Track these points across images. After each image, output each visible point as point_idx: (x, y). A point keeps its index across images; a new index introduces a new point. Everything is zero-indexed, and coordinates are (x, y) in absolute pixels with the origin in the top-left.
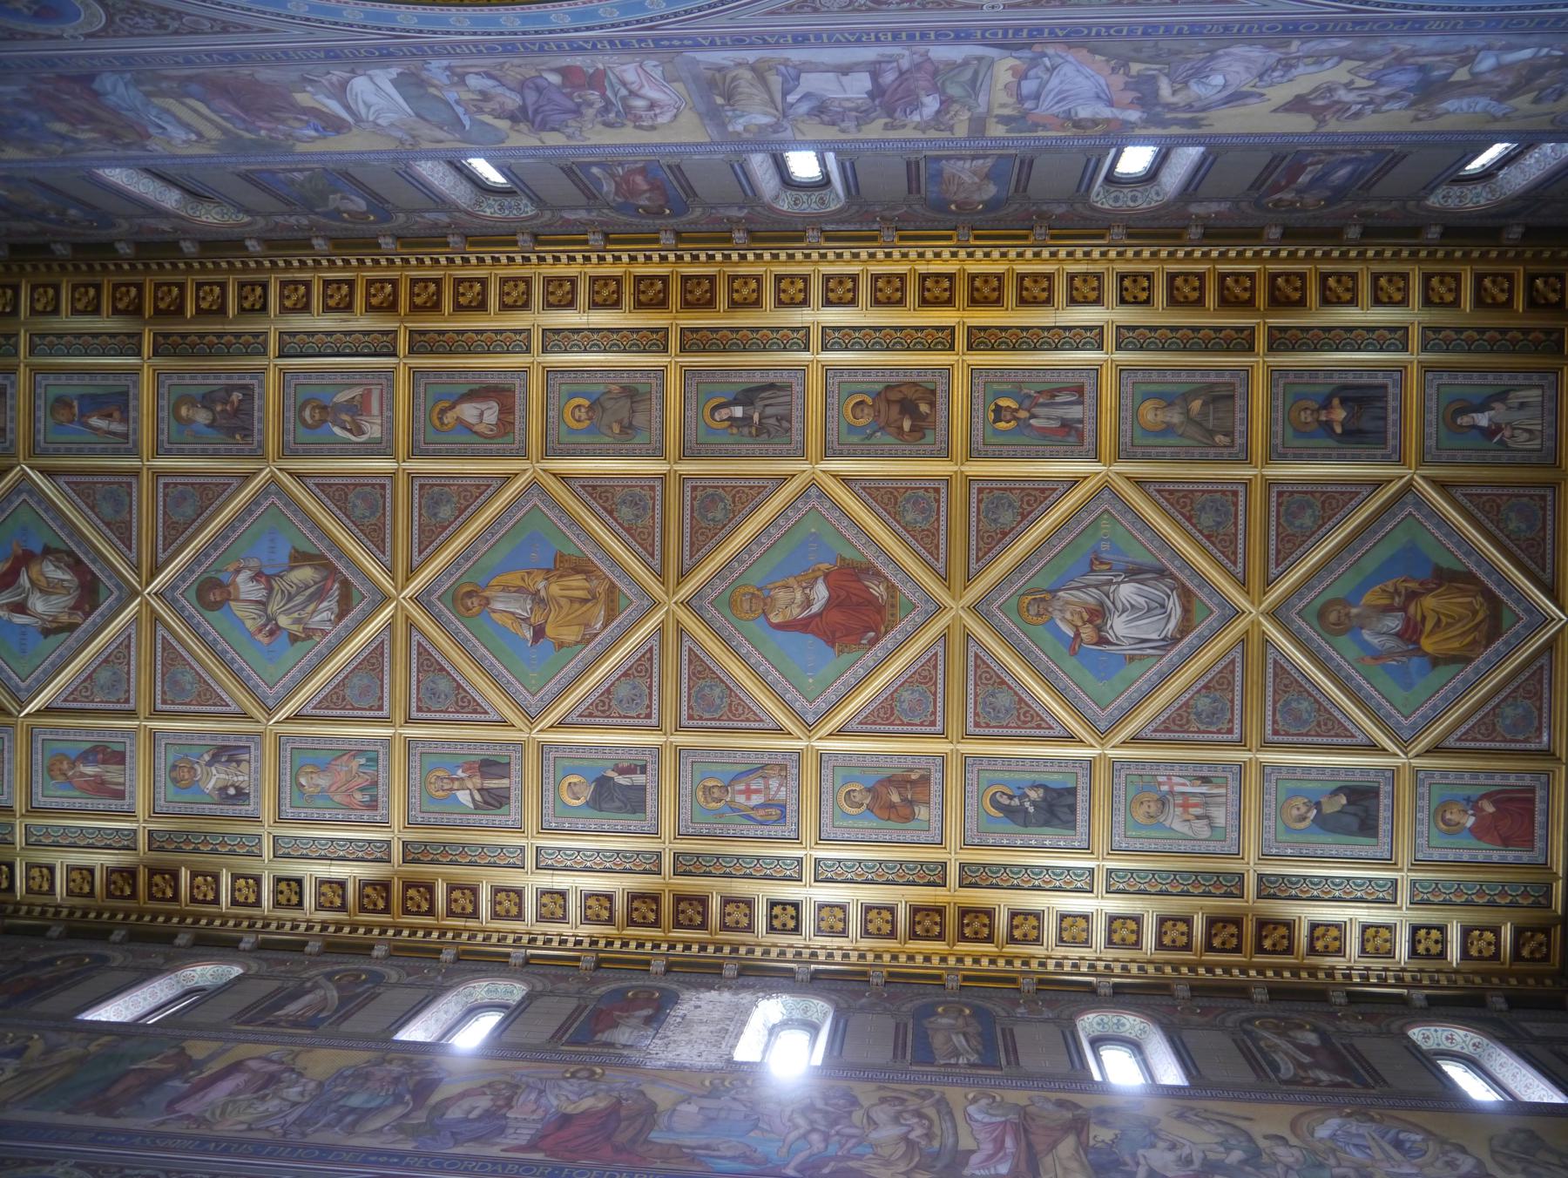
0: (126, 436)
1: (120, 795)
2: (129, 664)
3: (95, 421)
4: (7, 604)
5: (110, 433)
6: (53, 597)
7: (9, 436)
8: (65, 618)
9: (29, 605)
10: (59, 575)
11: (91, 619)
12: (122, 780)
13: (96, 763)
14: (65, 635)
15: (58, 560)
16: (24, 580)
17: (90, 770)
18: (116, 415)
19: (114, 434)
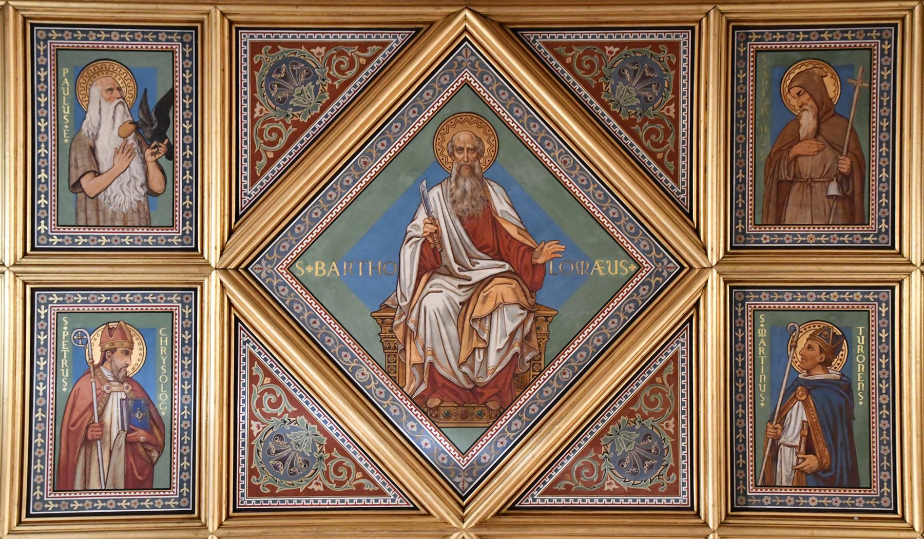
0: (769, 482)
1: (62, 482)
2: (327, 492)
3: (798, 415)
4: (438, 232)
5: (775, 449)
6: (453, 330)
7: (767, 234)
8: (413, 355)
9: (438, 280)
10: (497, 342)
11: (414, 412)
12: (94, 484)
13: (130, 425)
14: (380, 356)
15: (527, 338)
16: (485, 268)
17: (113, 414)
18: (811, 462)
19: (774, 458)
